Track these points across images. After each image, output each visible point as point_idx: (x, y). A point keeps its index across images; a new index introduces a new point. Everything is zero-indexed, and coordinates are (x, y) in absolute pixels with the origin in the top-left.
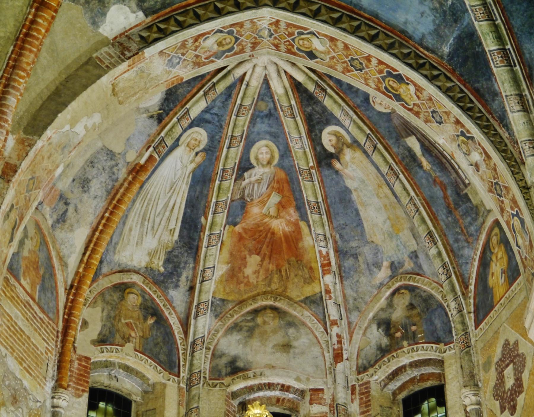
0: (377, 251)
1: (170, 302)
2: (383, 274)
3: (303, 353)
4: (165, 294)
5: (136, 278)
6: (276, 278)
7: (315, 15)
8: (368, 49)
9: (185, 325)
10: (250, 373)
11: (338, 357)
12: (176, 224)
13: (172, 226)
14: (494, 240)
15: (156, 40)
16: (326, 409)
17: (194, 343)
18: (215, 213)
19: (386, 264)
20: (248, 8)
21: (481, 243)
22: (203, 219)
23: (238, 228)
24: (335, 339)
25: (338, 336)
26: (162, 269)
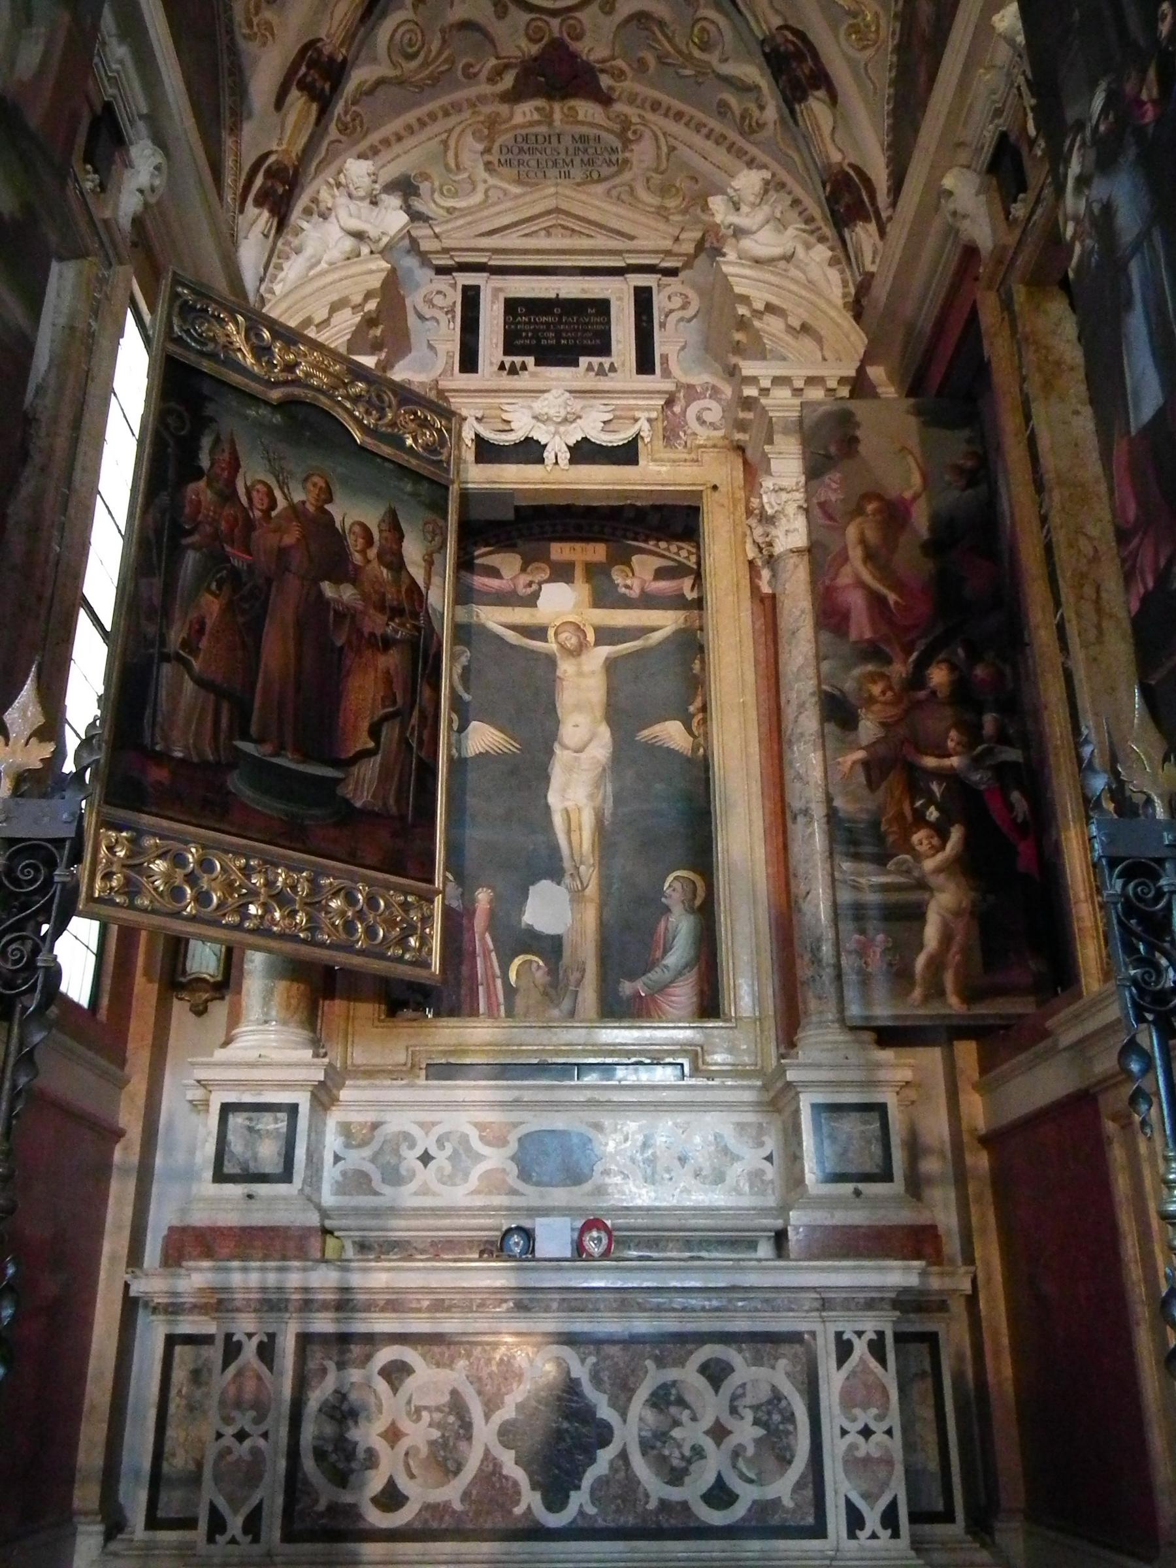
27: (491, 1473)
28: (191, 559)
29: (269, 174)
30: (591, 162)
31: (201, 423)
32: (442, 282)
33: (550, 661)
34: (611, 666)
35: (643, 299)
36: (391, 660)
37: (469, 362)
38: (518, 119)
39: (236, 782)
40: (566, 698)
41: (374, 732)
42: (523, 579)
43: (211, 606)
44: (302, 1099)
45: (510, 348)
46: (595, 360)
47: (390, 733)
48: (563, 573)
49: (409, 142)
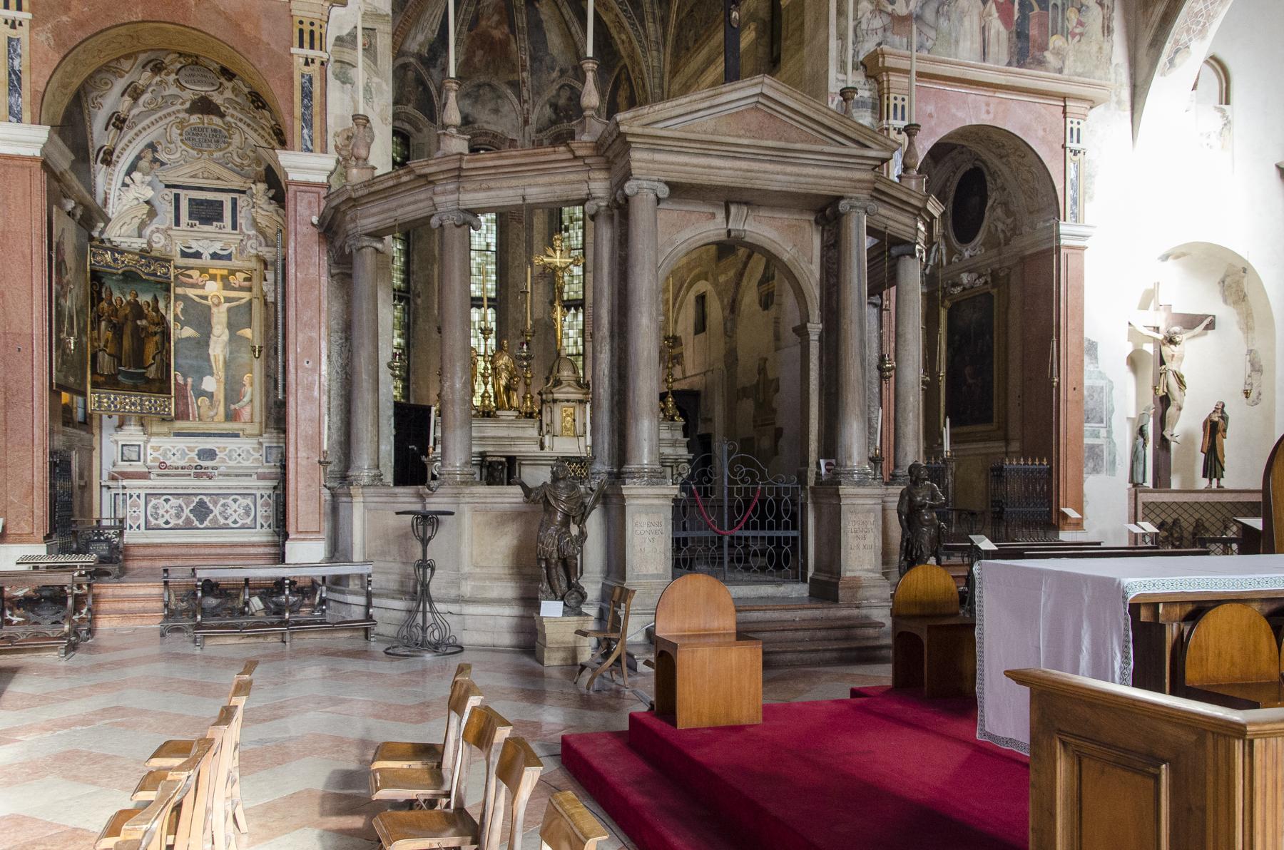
0: (554, 60)
1: (431, 76)
2: (555, 74)
3: (506, 116)
4: (428, 71)
6: (491, 66)
10: (476, 126)
11: (526, 122)
14: (623, 76)
19: (557, 69)
21: (616, 73)
27: (188, 518)
28: (103, 324)
29: (104, 153)
30: (217, 142)
31: (102, 285)
32: (167, 191)
33: (209, 308)
34: (229, 310)
35: (234, 202)
36: (157, 338)
37: (177, 223)
38: (192, 121)
39: (120, 377)
40: (214, 320)
41: (154, 358)
42: (201, 279)
43: (110, 334)
44: (142, 444)
45: (191, 215)
46: (219, 224)
47: (158, 358)
48: (213, 278)
49: (153, 128)
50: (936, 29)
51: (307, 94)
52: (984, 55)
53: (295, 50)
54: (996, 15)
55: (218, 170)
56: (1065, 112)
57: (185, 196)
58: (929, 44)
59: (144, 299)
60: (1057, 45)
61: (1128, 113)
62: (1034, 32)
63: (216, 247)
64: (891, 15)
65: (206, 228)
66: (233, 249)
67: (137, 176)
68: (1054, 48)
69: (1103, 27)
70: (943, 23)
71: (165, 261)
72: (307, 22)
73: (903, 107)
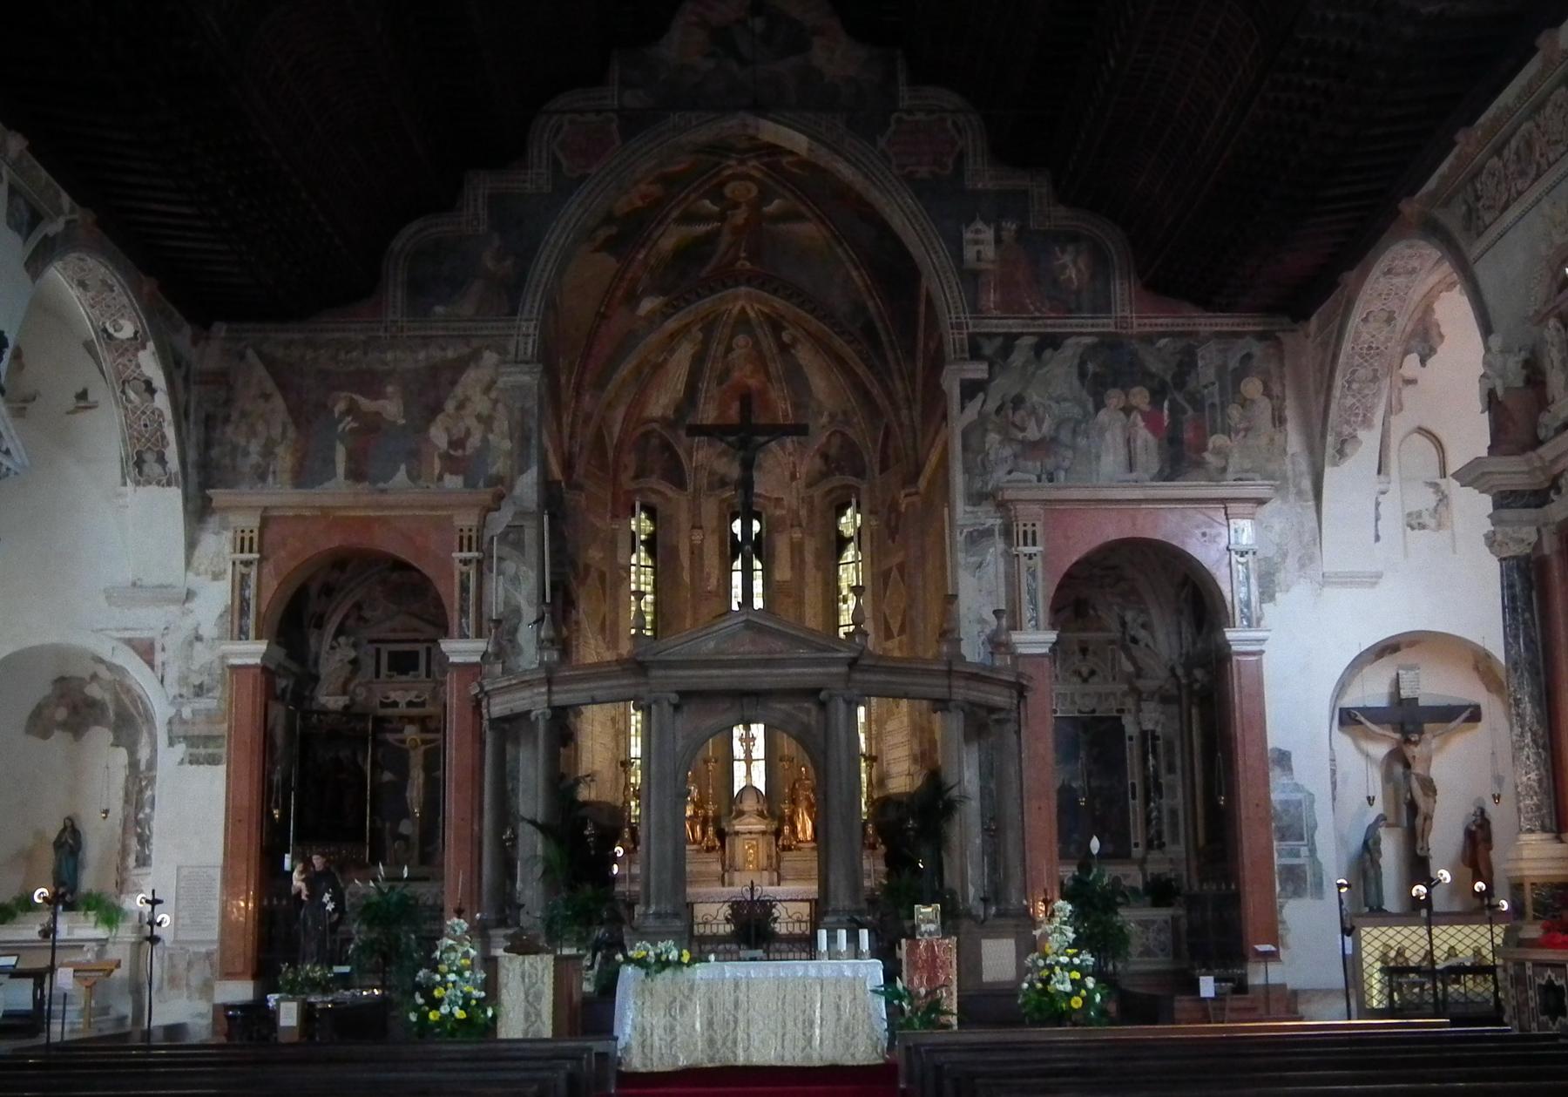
2: (824, 420)
5: (655, 426)
7: (775, 292)
8: (809, 317)
9: (690, 456)
11: (793, 477)
12: (681, 387)
13: (679, 386)
15: (672, 314)
16: (784, 512)
17: (696, 468)
18: (708, 383)
19: (826, 413)
20: (731, 287)
22: (700, 385)
23: (724, 386)
24: (791, 465)
25: (794, 464)
26: (672, 417)
32: (369, 646)
34: (426, 753)
37: (377, 675)
45: (390, 668)
50: (1074, 448)
51: (464, 589)
52: (1131, 467)
53: (454, 555)
54: (1142, 424)
55: (416, 623)
56: (1226, 514)
57: (385, 649)
58: (1066, 464)
59: (344, 754)
60: (1218, 444)
61: (1311, 503)
62: (1188, 435)
63: (411, 696)
64: (1022, 442)
65: (404, 678)
66: (427, 696)
67: (342, 640)
68: (1214, 447)
69: (1273, 418)
70: (1082, 442)
71: (362, 717)
72: (465, 529)
73: (1034, 533)
